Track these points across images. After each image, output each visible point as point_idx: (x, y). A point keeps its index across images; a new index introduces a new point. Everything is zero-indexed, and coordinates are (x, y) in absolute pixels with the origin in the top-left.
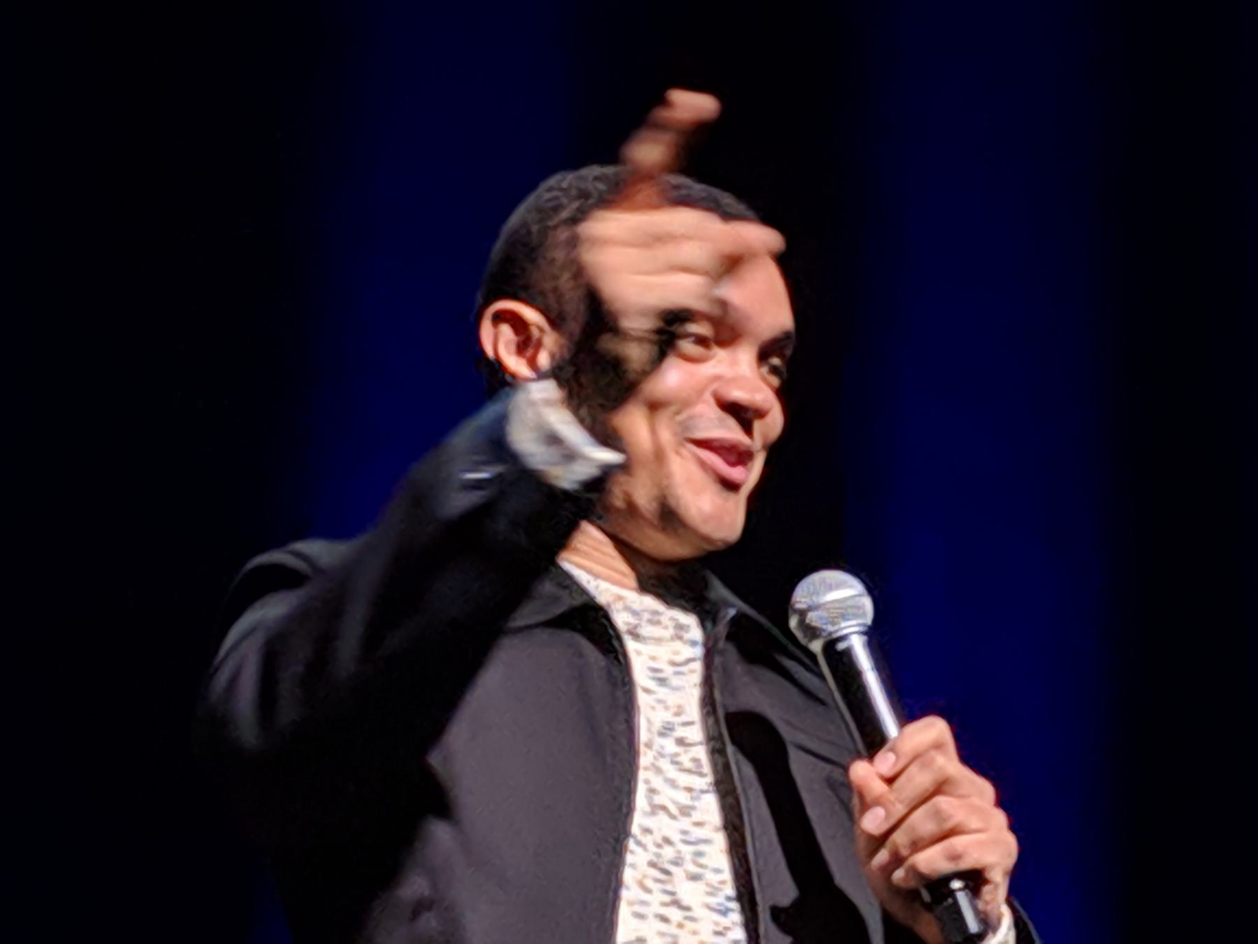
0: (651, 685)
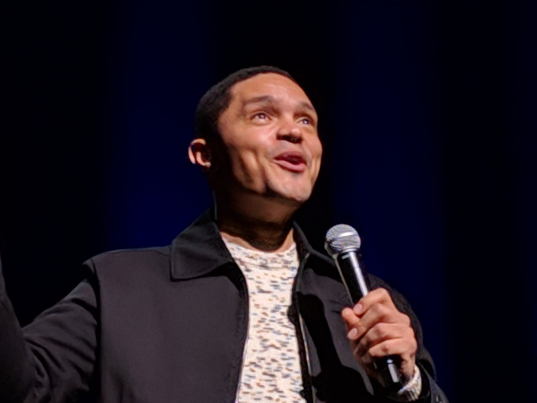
0: (271, 289)
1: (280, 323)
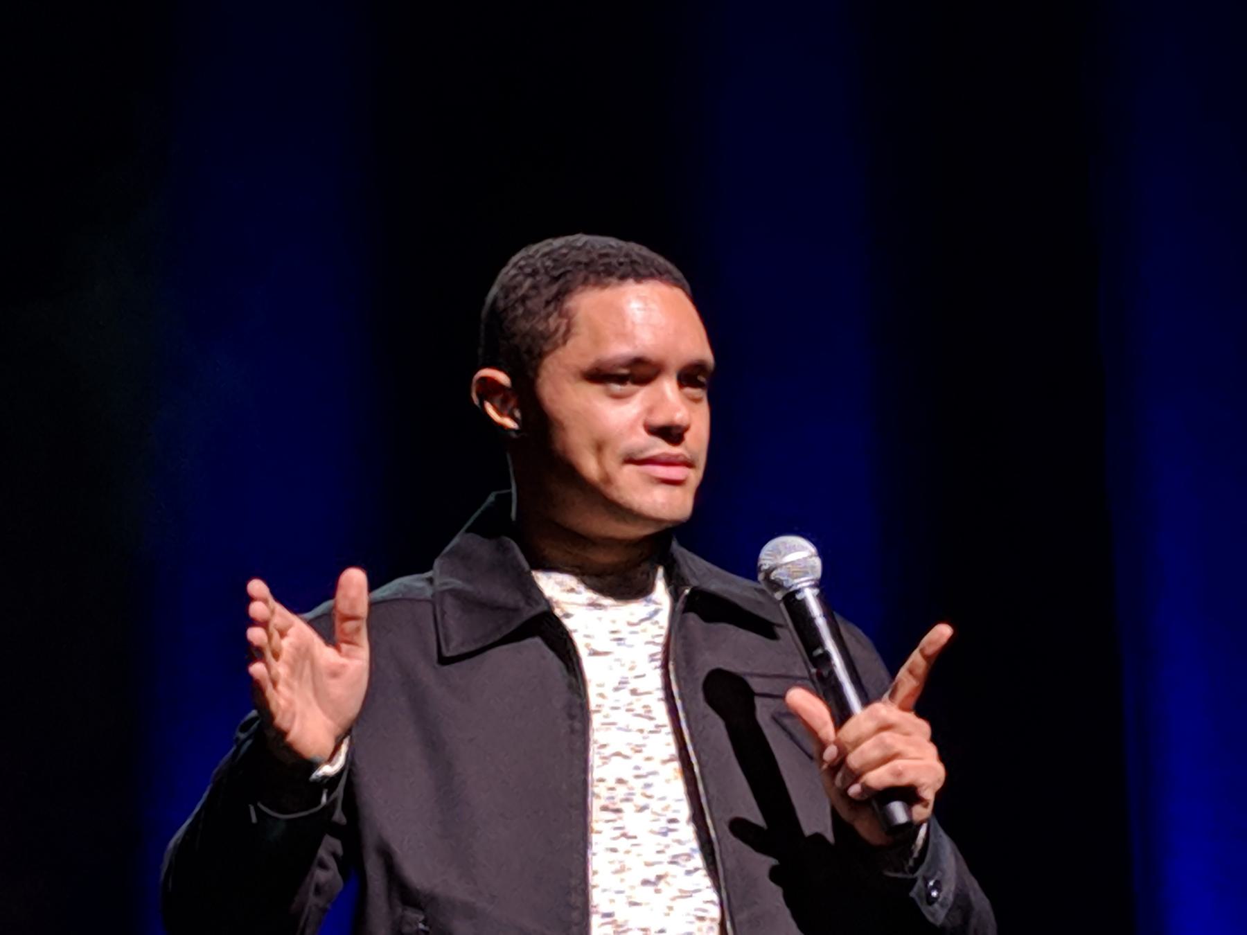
1: (628, 710)
